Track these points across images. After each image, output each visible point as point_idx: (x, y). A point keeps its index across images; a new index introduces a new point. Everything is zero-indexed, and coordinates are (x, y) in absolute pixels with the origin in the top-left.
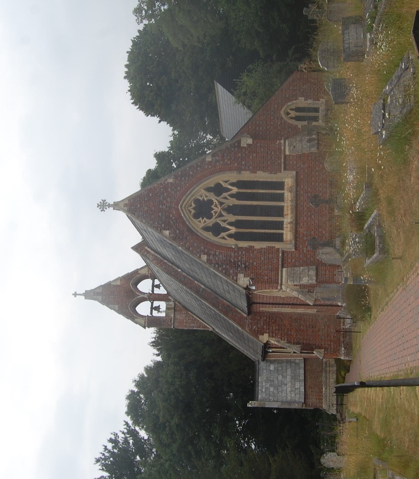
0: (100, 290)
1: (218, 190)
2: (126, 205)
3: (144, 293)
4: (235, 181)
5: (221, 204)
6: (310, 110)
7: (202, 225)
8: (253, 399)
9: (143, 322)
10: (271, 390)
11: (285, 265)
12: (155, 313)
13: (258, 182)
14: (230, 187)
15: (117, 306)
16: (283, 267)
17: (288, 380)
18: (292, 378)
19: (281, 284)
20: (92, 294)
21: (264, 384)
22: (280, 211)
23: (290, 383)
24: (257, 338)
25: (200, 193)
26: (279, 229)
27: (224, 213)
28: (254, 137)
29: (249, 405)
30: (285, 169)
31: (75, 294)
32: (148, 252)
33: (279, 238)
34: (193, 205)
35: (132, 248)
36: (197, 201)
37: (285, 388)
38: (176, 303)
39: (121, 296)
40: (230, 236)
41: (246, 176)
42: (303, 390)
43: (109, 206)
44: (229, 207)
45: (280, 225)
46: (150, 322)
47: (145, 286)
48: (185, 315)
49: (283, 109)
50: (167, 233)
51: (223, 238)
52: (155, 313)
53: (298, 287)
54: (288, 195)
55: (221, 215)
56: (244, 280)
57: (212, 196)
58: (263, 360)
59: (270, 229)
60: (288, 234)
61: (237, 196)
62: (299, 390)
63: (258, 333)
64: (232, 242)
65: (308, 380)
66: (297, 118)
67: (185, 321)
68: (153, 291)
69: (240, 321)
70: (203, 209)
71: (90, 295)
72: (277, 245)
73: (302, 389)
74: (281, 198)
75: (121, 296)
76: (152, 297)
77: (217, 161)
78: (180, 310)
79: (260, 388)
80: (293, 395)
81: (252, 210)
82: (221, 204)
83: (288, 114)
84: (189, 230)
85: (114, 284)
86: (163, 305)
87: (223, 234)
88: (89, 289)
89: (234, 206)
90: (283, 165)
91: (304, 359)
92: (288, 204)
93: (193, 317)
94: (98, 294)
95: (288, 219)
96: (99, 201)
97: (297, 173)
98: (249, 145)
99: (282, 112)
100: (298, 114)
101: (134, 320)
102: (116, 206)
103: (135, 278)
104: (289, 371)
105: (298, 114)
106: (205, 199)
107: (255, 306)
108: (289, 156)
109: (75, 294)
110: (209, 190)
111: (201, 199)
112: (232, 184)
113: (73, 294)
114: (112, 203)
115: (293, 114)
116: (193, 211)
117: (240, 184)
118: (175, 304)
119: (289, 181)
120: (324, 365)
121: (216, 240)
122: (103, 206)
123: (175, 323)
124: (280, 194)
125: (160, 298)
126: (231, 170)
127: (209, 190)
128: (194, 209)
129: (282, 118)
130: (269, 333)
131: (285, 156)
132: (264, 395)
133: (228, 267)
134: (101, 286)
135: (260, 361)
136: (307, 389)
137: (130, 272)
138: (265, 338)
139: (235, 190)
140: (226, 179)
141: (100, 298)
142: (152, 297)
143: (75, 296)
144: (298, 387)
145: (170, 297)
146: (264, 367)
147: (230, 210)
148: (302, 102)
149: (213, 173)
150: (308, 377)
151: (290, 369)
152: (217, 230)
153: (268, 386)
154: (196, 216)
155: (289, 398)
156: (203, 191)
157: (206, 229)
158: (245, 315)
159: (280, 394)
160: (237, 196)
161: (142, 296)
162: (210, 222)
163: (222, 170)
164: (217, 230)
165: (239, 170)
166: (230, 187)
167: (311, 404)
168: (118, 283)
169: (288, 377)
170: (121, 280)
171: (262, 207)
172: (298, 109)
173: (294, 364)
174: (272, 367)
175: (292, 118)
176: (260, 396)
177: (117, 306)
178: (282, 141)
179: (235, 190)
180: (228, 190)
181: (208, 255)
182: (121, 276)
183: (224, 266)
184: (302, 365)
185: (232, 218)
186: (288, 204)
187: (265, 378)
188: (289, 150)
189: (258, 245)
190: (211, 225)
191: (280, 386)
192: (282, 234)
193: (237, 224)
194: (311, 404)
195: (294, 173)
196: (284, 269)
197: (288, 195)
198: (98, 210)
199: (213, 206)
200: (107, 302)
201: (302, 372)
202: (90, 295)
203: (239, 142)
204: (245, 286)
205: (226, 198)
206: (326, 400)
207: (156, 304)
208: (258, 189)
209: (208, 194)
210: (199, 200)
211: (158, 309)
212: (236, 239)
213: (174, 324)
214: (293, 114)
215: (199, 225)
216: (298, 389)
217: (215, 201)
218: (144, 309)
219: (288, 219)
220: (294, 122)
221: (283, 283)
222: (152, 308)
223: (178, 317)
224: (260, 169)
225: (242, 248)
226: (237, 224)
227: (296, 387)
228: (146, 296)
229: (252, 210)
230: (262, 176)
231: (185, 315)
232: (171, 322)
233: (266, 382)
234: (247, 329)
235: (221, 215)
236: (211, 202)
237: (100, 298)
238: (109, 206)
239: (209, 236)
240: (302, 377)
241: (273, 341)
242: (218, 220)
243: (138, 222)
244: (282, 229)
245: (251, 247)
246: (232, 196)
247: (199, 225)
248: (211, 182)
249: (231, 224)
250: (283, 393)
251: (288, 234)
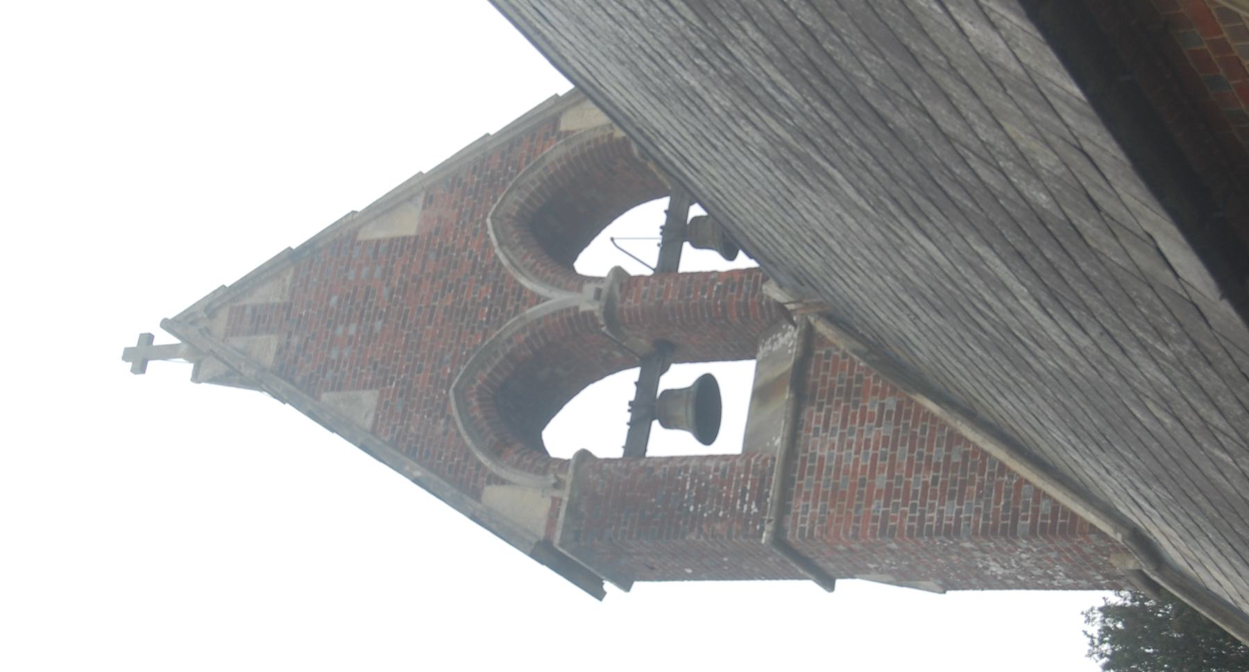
0: (269, 294)
15: (369, 398)
20: (221, 324)
38: (822, 328)
48: (886, 430)
52: (670, 443)
67: (881, 481)
85: (380, 234)
86: (736, 380)
93: (955, 438)
94: (260, 320)
101: (477, 495)
109: (141, 355)
113: (128, 354)
118: (809, 338)
123: (798, 504)
125: (720, 321)
134: (290, 256)
137: (493, 131)
141: (266, 347)
143: (140, 368)
168: (408, 224)
170: (429, 200)
177: (369, 398)
182: (427, 163)
200: (303, 379)
213: (783, 508)
218: (593, 421)
222: (649, 409)
223: (823, 446)
231: (886, 430)
232: (760, 499)
237: (266, 347)
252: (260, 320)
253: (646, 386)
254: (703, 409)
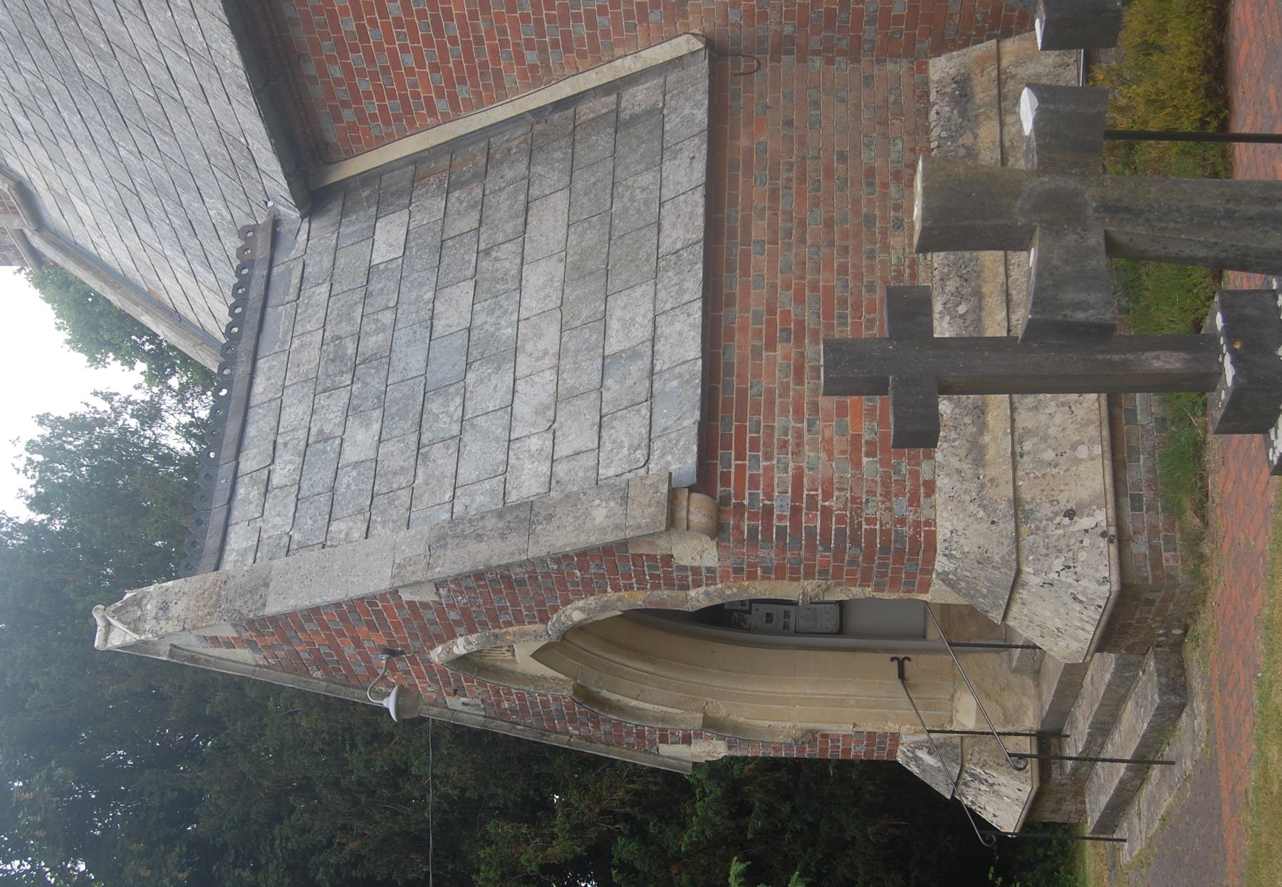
10: (350, 455)
17: (531, 303)
18: (576, 272)
21: (295, 413)
23: (552, 331)
29: (114, 635)
37: (488, 391)
42: (692, 348)
62: (638, 369)
65: (759, 260)
73: (683, 342)
80: (576, 436)
91: (717, 51)
104: (550, 222)
120: (940, 109)
132: (277, 521)
135: (291, 214)
136: (739, 349)
144: (641, 332)
146: (319, 264)
150: (759, 229)
151: (559, 201)
153: (330, 418)
155: (529, 481)
159: (442, 458)
167: (781, 505)
169: (534, 278)
173: (603, 141)
174: (389, 236)
176: (238, 540)
187: (309, 358)
191: (441, 389)
194: (781, 505)
201: (686, 173)
206: (977, 454)
216: (633, 354)
227: (613, 346)
233: (320, 387)
240: (684, 226)
250: (473, 446)
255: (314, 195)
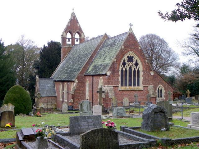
0: (75, 19)
1: (137, 64)
2: (131, 33)
3: (75, 35)
4: (139, 70)
5: (132, 65)
6: (161, 94)
7: (126, 59)
8: (39, 77)
9: (65, 34)
11: (114, 87)
12: (67, 40)
13: (139, 78)
14: (138, 68)
15: (69, 25)
16: (113, 86)
19: (108, 86)
20: (74, 16)
22: (130, 85)
24: (76, 79)
25: (136, 58)
26: (125, 85)
27: (129, 66)
28: (153, 76)
29: (37, 76)
30: (144, 86)
31: (73, 9)
32: (104, 39)
33: (122, 85)
34: (132, 56)
35: (106, 33)
36: (133, 57)
39: (73, 26)
40: (122, 69)
41: (141, 74)
43: (131, 27)
44: (131, 68)
45: (126, 85)
46: (64, 38)
47: (77, 36)
49: (162, 86)
50: (123, 47)
51: (121, 66)
52: (67, 40)
53: (107, 92)
54: (136, 88)
55: (129, 65)
56: (108, 74)
57: (134, 62)
58: (54, 81)
59: (125, 82)
60: (124, 88)
61: (135, 71)
63: (78, 78)
64: (120, 69)
66: (158, 90)
68: (75, 39)
69: (81, 73)
70: (130, 59)
71: (73, 15)
72: (120, 84)
74: (134, 85)
75: (73, 26)
76: (73, 39)
77: (146, 64)
78: (69, 49)
79: (43, 80)
81: (130, 76)
82: (132, 65)
83: (160, 87)
84: (124, 55)
86: (70, 43)
87: (123, 66)
88: (76, 14)
89: (132, 70)
90: (145, 86)
92: (132, 87)
94: (74, 18)
95: (128, 88)
96: (132, 23)
97: (142, 91)
98: (151, 74)
99: (160, 85)
100: (160, 90)
102: (131, 29)
103: (80, 32)
105: (160, 90)
106: (134, 60)
107: (92, 77)
108: (148, 88)
109: (73, 9)
110: (136, 61)
111: (134, 58)
112: (138, 69)
114: (132, 28)
115: (160, 89)
116: (130, 56)
117: (138, 71)
119: (141, 87)
121: (121, 64)
122: (131, 25)
124: (136, 85)
126: (143, 68)
127: (136, 61)
128: (130, 56)
129: (159, 85)
130: (78, 82)
131: (148, 86)
133: (113, 68)
138: (77, 81)
139: (137, 70)
140: (140, 67)
141: (73, 18)
142: (73, 39)
145: (74, 45)
147: (130, 68)
148: (164, 91)
149: (142, 62)
152: (124, 64)
154: (128, 57)
156: (136, 59)
157: (124, 60)
158: (84, 74)
160: (135, 71)
161: (74, 35)
162: (126, 62)
163: (143, 65)
164: (124, 64)
165: (143, 71)
166: (138, 68)
168: (78, 26)
171: (131, 79)
172: (161, 90)
175: (159, 88)
178: (152, 85)
179: (137, 70)
180: (136, 67)
181: (116, 61)
183: (113, 67)
184: (54, 95)
185: (128, 69)
186: (132, 87)
188: (150, 88)
189: (120, 78)
190: (125, 62)
192: (123, 86)
193: (126, 71)
195: (143, 90)
196: (112, 87)
197: (136, 88)
198: (129, 23)
199: (131, 62)
202: (73, 15)
203: (152, 71)
204: (107, 74)
205: (134, 67)
207: (71, 40)
208: (137, 78)
209: (135, 60)
210: (133, 58)
211: (69, 41)
212: (121, 71)
214: (160, 89)
215: (125, 57)
217: (133, 63)
218: (69, 36)
219: (128, 88)
220: (157, 89)
221: (109, 87)
222: (69, 39)
223: (67, 48)
224: (144, 78)
225: (119, 72)
226: (126, 71)
228: (74, 36)
229: (130, 76)
230: (141, 79)
234: (79, 75)
235: (129, 65)
236: (133, 62)
237: (73, 18)
238: (131, 27)
239: (122, 62)
241: (75, 84)
242: (127, 65)
243: (125, 37)
244: (125, 86)
245: (119, 76)
246: (135, 69)
247: (125, 57)
248: (139, 62)
249: (126, 69)
251: (124, 88)
252: (74, 18)
253: (70, 38)
254: (69, 41)
255: (54, 81)
